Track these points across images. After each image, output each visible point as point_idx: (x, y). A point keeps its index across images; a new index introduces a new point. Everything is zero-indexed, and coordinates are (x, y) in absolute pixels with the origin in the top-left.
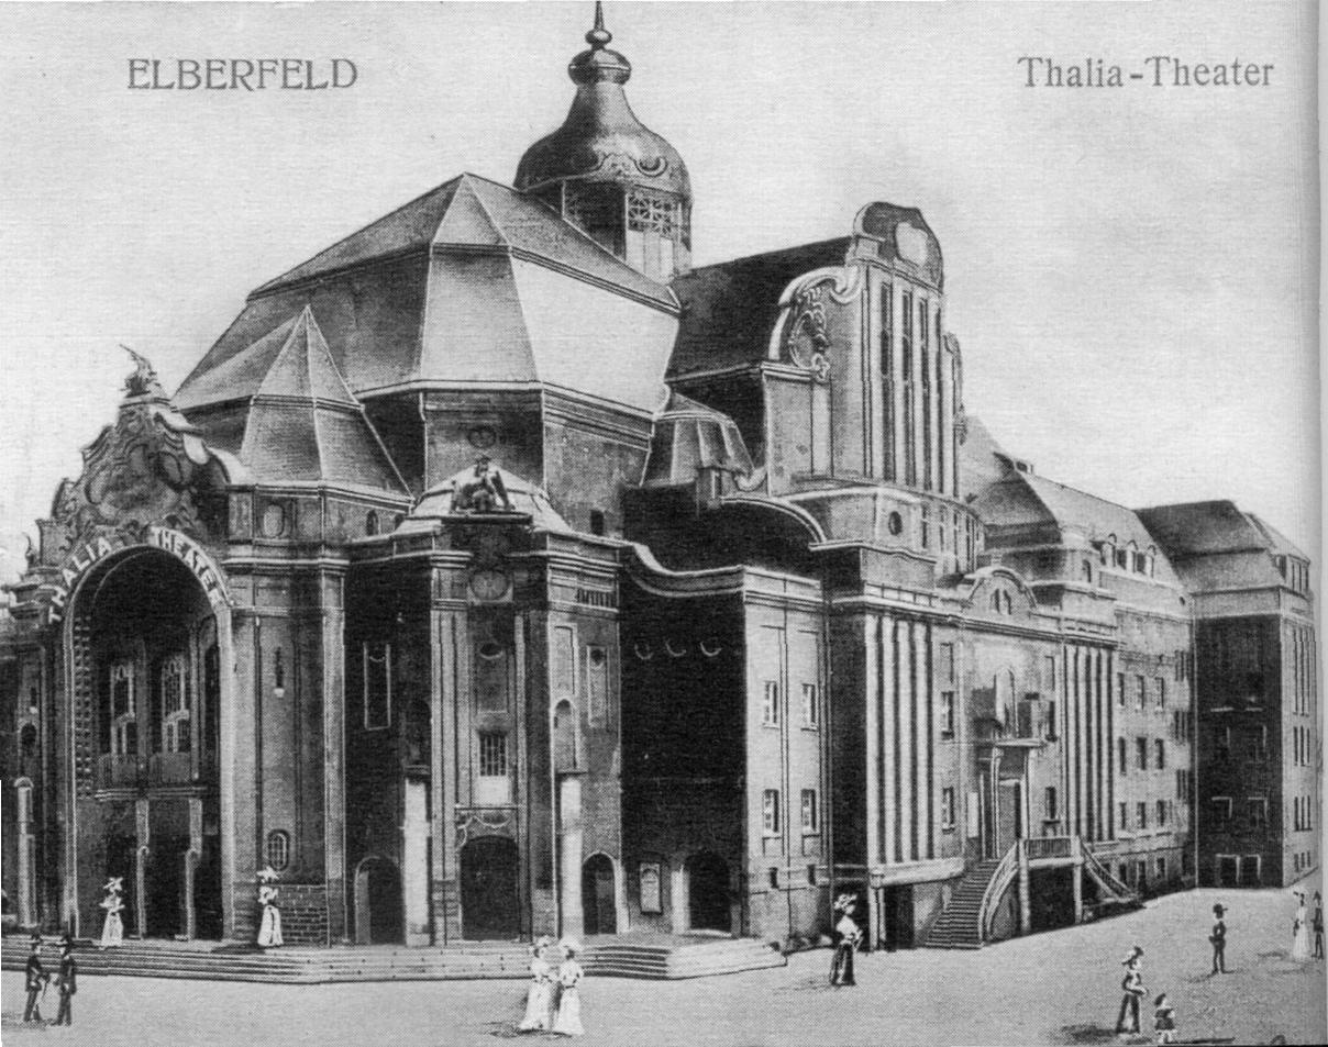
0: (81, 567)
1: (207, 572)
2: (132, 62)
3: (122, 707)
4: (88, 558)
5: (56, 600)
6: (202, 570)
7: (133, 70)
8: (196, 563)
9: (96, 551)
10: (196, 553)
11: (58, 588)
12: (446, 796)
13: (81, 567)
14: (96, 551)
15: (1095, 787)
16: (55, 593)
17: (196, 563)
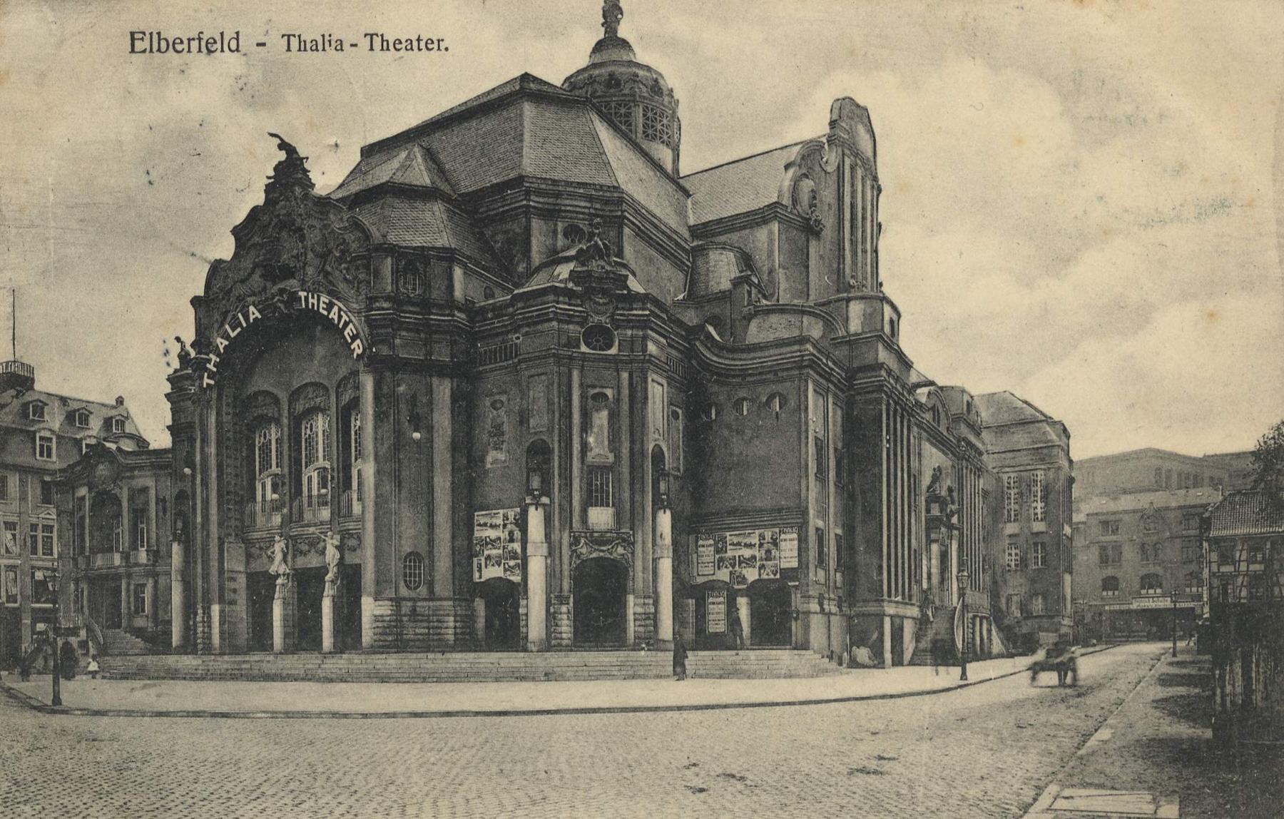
0: (233, 335)
1: (351, 326)
2: (132, 34)
3: (266, 464)
4: (240, 324)
5: (211, 366)
6: (346, 324)
7: (133, 39)
8: (340, 317)
9: (247, 319)
10: (340, 309)
11: (211, 356)
12: (162, 705)
13: (233, 335)
14: (247, 319)
15: (892, 470)
16: (209, 361)
17: (340, 317)
